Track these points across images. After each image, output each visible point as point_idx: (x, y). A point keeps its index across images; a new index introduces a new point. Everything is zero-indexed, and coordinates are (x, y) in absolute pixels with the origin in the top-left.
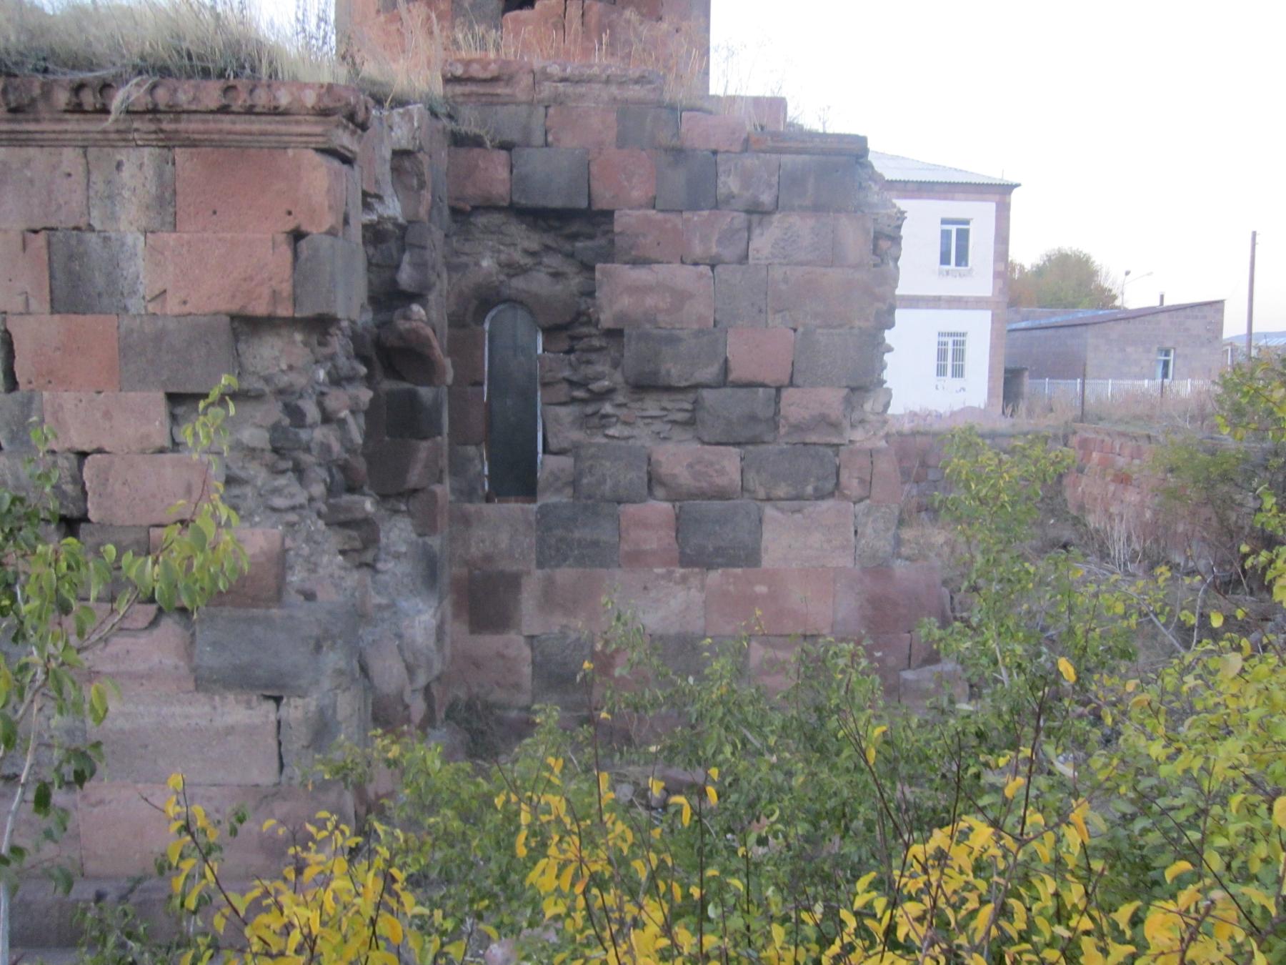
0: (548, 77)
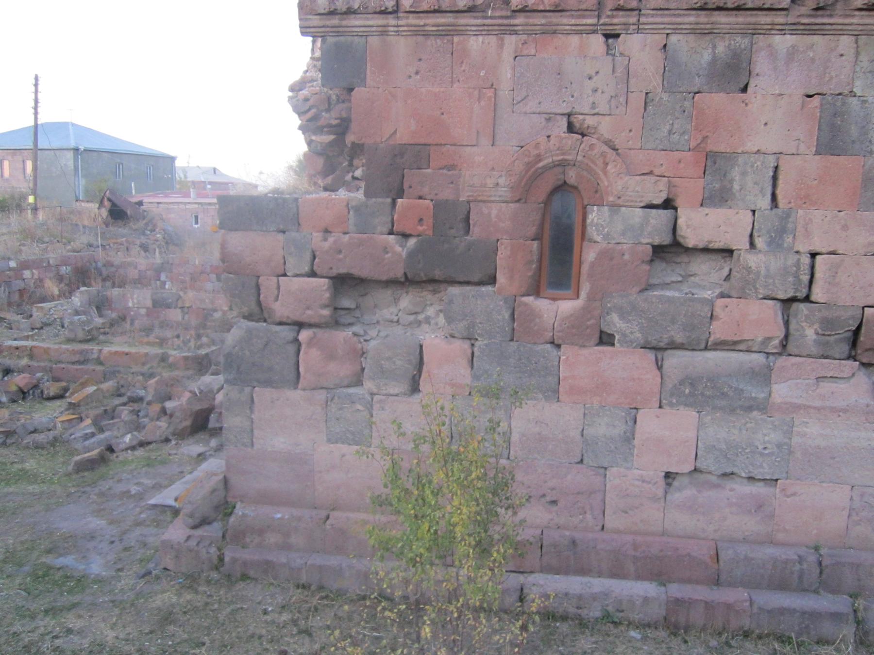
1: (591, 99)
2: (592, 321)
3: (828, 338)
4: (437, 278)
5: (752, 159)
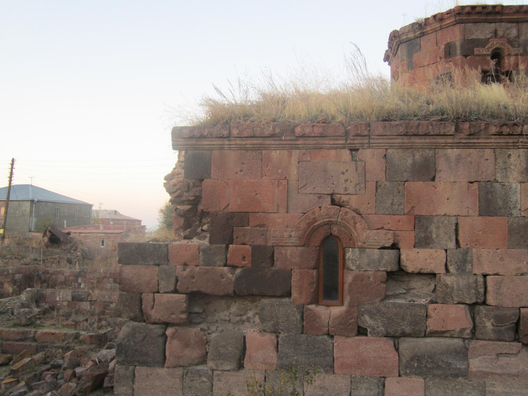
1: (344, 186)
2: (353, 320)
3: (500, 328)
4: (254, 293)
5: (442, 219)
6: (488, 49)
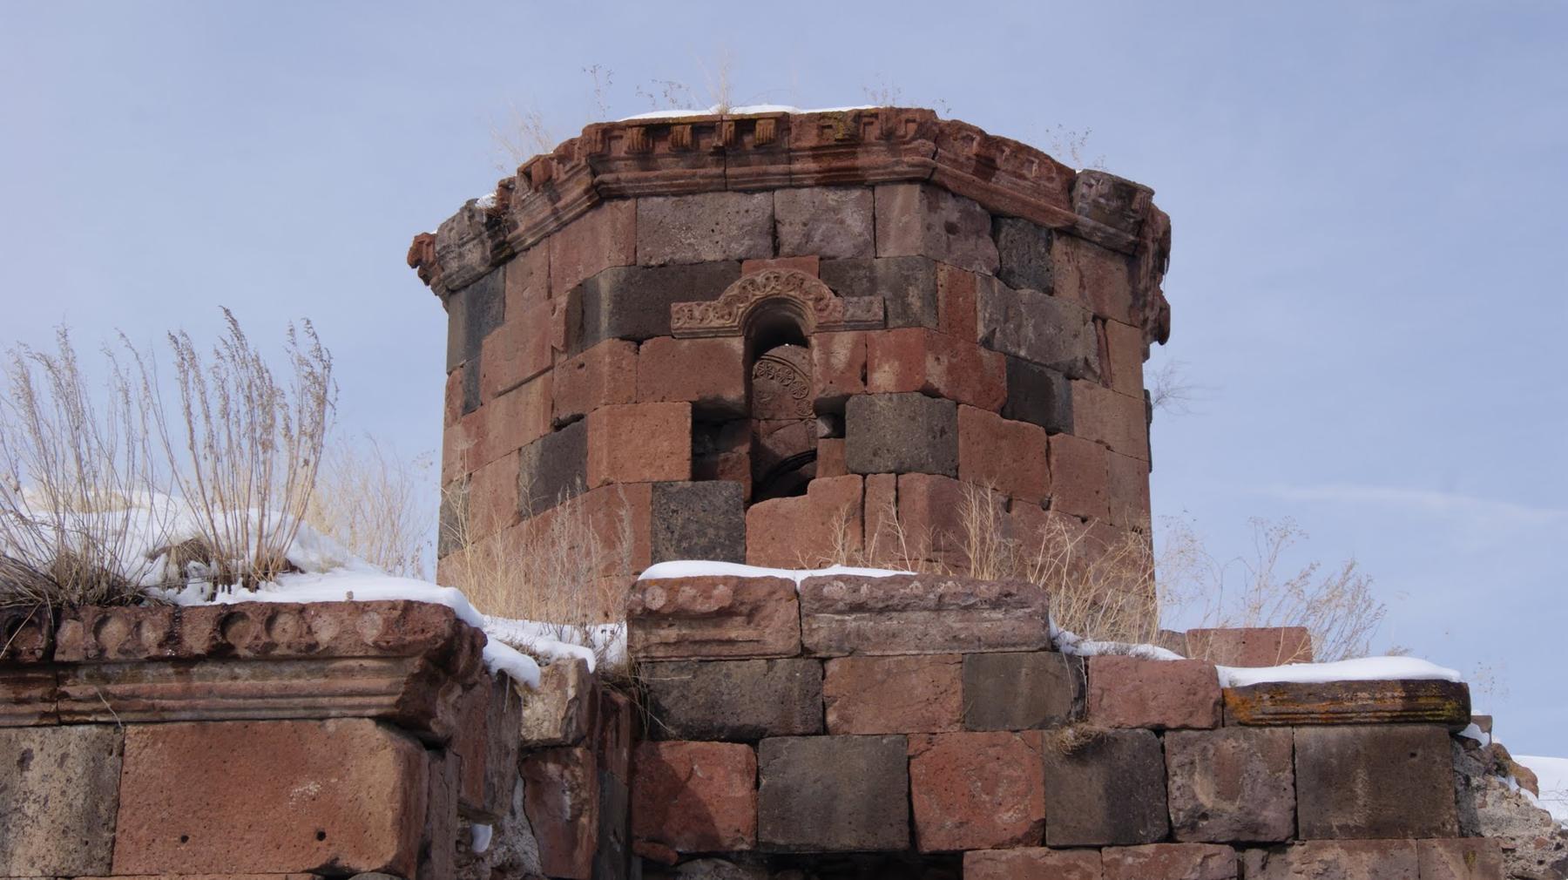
0: (826, 605)
6: (728, 304)
